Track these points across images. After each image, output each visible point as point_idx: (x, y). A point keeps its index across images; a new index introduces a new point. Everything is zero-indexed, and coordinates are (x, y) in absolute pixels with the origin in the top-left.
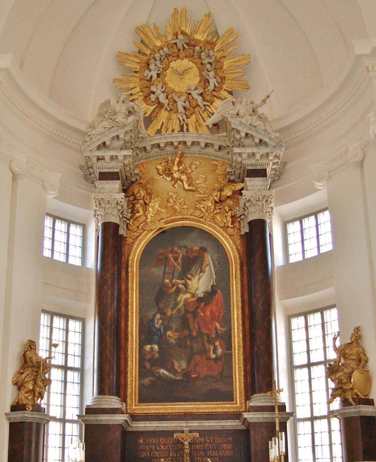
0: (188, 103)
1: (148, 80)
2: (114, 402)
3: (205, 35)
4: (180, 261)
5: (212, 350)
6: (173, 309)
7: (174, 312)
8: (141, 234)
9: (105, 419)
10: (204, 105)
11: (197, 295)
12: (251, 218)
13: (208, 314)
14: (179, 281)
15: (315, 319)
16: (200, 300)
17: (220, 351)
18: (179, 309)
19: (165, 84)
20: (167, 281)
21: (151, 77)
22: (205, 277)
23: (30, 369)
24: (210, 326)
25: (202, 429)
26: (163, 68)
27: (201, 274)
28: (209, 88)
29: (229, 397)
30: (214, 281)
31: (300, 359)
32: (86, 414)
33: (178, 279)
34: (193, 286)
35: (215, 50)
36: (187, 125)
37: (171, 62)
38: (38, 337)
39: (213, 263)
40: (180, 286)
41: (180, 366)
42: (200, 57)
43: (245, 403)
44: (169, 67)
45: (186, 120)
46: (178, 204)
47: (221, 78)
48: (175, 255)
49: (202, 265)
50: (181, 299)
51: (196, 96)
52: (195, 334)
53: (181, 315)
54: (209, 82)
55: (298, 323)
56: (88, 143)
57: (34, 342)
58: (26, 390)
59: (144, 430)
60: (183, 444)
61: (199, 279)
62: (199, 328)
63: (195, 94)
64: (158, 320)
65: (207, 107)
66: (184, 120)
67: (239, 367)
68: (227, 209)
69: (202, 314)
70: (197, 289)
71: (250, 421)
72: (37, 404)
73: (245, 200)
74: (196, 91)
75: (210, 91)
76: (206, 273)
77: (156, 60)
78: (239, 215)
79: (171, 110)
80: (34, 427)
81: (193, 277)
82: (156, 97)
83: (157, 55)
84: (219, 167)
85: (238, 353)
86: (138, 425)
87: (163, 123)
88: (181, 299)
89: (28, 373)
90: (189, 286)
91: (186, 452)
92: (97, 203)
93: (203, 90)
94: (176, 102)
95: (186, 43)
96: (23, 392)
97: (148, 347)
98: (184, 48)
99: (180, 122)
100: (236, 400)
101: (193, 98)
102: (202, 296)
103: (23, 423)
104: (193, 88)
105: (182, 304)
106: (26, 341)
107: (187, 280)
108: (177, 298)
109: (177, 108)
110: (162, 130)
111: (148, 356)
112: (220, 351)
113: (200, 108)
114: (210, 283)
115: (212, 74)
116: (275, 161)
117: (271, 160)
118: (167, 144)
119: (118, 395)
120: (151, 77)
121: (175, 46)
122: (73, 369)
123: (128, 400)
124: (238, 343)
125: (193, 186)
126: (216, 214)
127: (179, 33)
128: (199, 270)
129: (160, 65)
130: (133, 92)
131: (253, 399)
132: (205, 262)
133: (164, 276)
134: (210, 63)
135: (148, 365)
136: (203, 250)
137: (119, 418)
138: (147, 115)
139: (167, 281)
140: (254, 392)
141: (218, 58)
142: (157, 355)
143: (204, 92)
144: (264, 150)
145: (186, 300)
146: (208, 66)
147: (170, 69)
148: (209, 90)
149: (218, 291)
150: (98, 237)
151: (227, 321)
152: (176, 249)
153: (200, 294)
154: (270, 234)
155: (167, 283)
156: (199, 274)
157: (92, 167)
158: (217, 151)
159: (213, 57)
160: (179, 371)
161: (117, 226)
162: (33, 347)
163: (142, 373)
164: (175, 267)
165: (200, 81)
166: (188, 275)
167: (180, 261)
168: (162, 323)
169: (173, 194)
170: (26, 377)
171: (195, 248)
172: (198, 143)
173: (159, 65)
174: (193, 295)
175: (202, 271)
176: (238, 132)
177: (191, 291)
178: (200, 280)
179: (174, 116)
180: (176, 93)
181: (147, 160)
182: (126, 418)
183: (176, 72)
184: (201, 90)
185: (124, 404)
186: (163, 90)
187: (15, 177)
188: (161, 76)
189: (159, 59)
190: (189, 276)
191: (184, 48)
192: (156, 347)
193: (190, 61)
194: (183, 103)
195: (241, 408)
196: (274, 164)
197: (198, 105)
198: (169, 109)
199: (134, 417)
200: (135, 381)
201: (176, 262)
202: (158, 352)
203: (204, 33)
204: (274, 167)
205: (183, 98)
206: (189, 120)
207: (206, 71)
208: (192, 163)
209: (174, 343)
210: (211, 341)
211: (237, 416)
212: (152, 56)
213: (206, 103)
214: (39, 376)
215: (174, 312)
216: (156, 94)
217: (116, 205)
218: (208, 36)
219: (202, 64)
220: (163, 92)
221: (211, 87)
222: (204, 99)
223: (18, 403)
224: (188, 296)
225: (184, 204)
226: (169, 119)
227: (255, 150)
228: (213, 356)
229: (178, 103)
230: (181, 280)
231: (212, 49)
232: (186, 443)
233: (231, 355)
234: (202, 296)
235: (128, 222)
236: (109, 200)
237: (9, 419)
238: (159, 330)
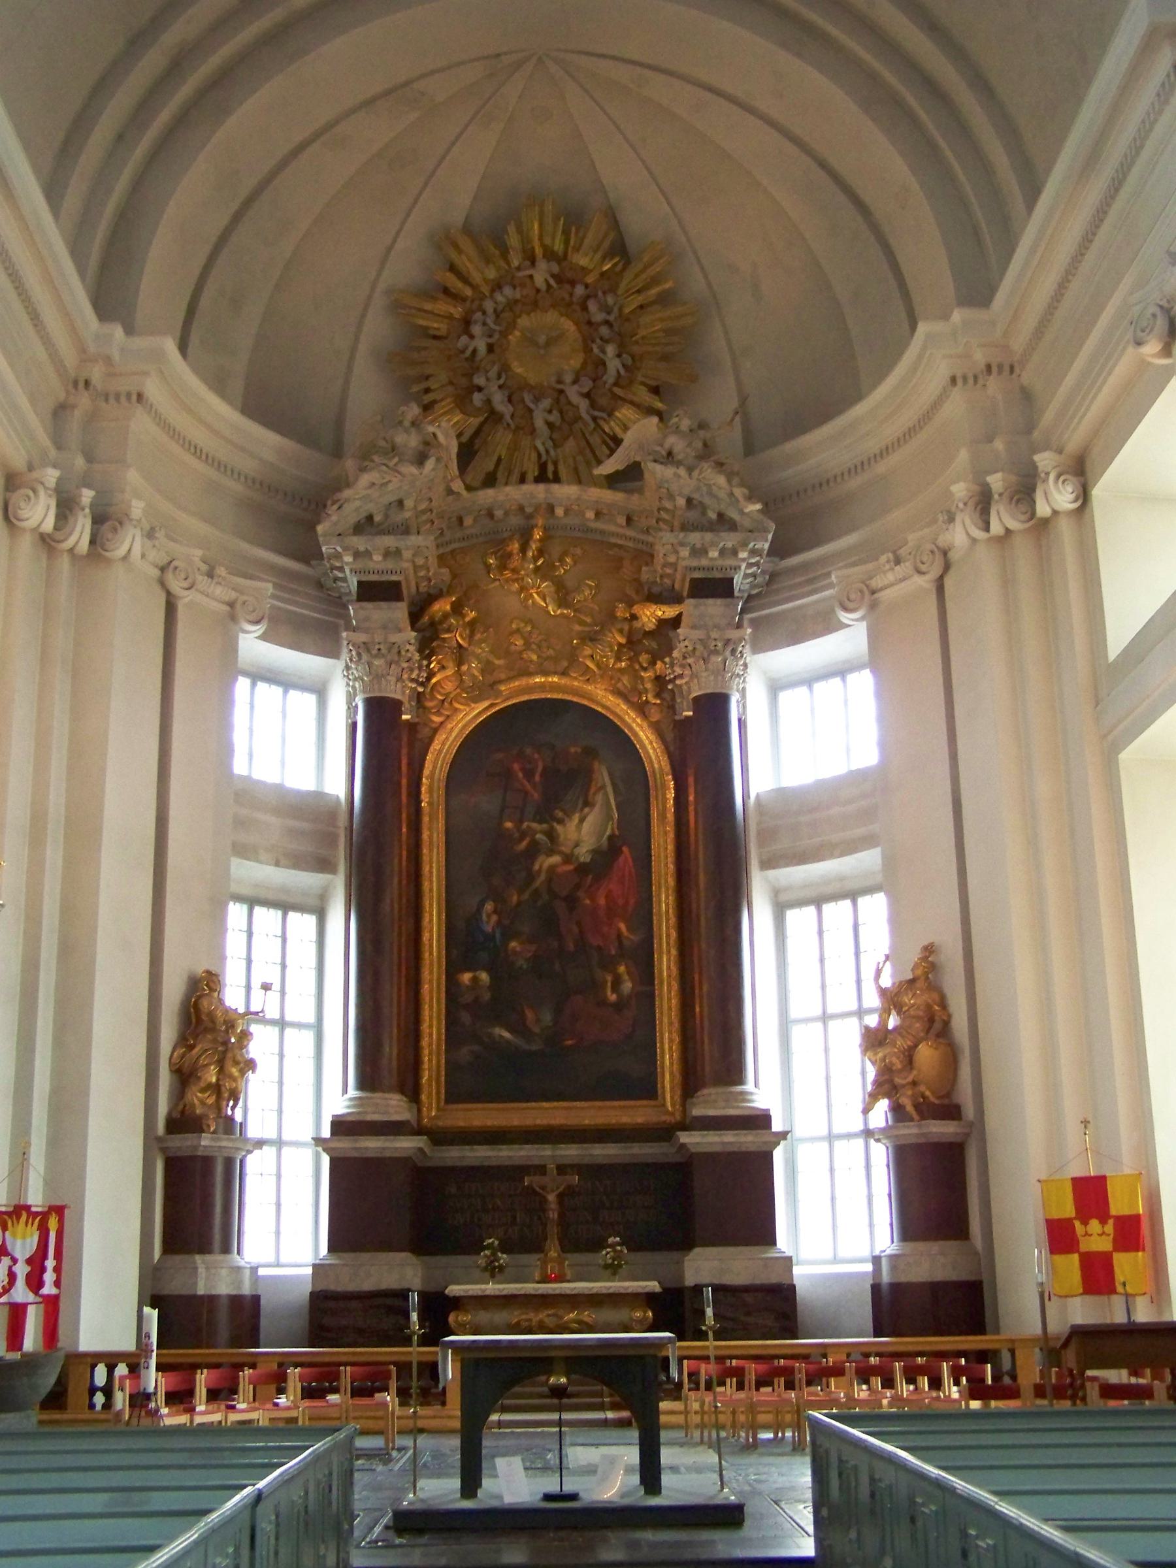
0: (559, 415)
1: (467, 359)
2: (395, 1107)
3: (598, 256)
4: (537, 778)
5: (609, 984)
6: (521, 891)
7: (526, 896)
8: (448, 717)
9: (372, 1145)
10: (595, 419)
11: (577, 858)
13: (602, 901)
14: (535, 825)
15: (838, 912)
16: (582, 869)
17: (627, 986)
18: (536, 890)
19: (505, 369)
20: (509, 825)
21: (474, 351)
22: (593, 818)
23: (209, 1037)
24: (605, 929)
25: (586, 1161)
26: (500, 332)
27: (586, 810)
28: (604, 378)
29: (648, 1090)
30: (615, 826)
31: (804, 1003)
32: (333, 1133)
33: (534, 821)
34: (569, 837)
35: (620, 292)
36: (555, 463)
37: (520, 316)
38: (223, 958)
39: (614, 785)
40: (538, 836)
41: (538, 1021)
42: (585, 308)
43: (684, 1105)
44: (514, 328)
45: (552, 453)
46: (534, 647)
47: (633, 357)
48: (528, 766)
49: (588, 790)
50: (541, 867)
51: (575, 399)
52: (571, 947)
53: (540, 903)
54: (604, 364)
55: (800, 919)
56: (334, 518)
57: (217, 975)
58: (202, 1084)
59: (459, 1164)
60: (546, 1200)
61: (582, 820)
62: (581, 932)
63: (573, 394)
64: (489, 916)
65: (601, 423)
66: (547, 452)
67: (671, 1024)
68: (644, 658)
69: (588, 902)
70: (577, 845)
71: (693, 1150)
72: (227, 1117)
73: (684, 650)
74: (576, 387)
75: (607, 386)
76: (597, 809)
77: (484, 313)
78: (672, 676)
79: (518, 428)
80: (219, 1169)
81: (568, 816)
82: (485, 398)
84: (626, 563)
85: (669, 992)
86: (447, 1155)
87: (499, 460)
88: (541, 867)
89: (206, 1045)
90: (558, 836)
91: (551, 1216)
92: (354, 653)
93: (591, 383)
94: (530, 411)
95: (553, 276)
96: (194, 1088)
97: (466, 977)
98: (549, 286)
99: (539, 456)
100: (664, 1098)
101: (569, 403)
102: (588, 860)
103: (193, 1158)
104: (568, 378)
105: (543, 877)
106: (200, 970)
107: (555, 824)
108: (533, 864)
109: (533, 424)
110: (499, 475)
111: (468, 998)
112: (627, 986)
113: (586, 424)
114: (605, 831)
115: (611, 350)
116: (753, 561)
117: (743, 560)
119: (401, 1090)
120: (474, 351)
121: (528, 281)
122: (299, 1026)
123: (424, 1097)
124: (669, 968)
125: (567, 606)
126: (621, 670)
127: (539, 251)
128: (581, 802)
129: (495, 324)
130: (431, 383)
131: (701, 1099)
132: (593, 783)
133: (502, 810)
134: (607, 323)
135: (465, 1017)
136: (590, 753)
137: (406, 1145)
138: (464, 439)
139: (509, 825)
140: (704, 1086)
141: (627, 310)
142: (487, 996)
143: (594, 387)
145: (552, 868)
146: (604, 331)
147: (517, 333)
148: (605, 383)
149: (625, 849)
150: (354, 725)
151: (645, 918)
152: (528, 751)
153: (583, 854)
154: (740, 720)
155: (508, 829)
156: (582, 810)
157: (341, 569)
158: (622, 527)
159: (616, 310)
160: (536, 1030)
161: (395, 706)
162: (212, 985)
163: (454, 1035)
164: (526, 793)
165: (584, 364)
166: (557, 811)
167: (537, 778)
168: (499, 923)
169: (522, 625)
170: (200, 1056)
171: (573, 750)
173: (492, 325)
174: (568, 859)
175: (587, 803)
177: (563, 849)
178: (586, 825)
179: (525, 442)
180: (531, 388)
181: (463, 544)
182: (421, 1145)
183: (530, 340)
184: (586, 385)
185: (415, 1106)
186: (501, 382)
188: (495, 347)
189: (492, 310)
190: (560, 814)
191: (549, 286)
192: (484, 976)
193: (562, 315)
194: (546, 414)
195: (672, 1114)
196: (750, 565)
197: (578, 418)
198: (513, 426)
199: (440, 1137)
200: (438, 1054)
201: (529, 781)
202: (490, 988)
203: (595, 251)
204: (750, 571)
205: (546, 403)
206: (559, 450)
207: (598, 341)
208: (565, 553)
209: (525, 967)
210: (608, 964)
211: (664, 1133)
212: (477, 303)
213: (596, 413)
214: (229, 1055)
215: (526, 896)
216: (486, 391)
217: (396, 658)
218: (604, 258)
219: (589, 323)
220: (500, 387)
221: (610, 377)
222: (593, 405)
223: (183, 1112)
224: (555, 859)
225: (548, 648)
226: (514, 447)
228: (613, 997)
229: (535, 414)
230: (540, 822)
231: (613, 290)
232: (551, 1197)
233: (651, 996)
234: (588, 860)
235: (421, 689)
236: (382, 647)
237: (163, 1150)
238: (490, 938)
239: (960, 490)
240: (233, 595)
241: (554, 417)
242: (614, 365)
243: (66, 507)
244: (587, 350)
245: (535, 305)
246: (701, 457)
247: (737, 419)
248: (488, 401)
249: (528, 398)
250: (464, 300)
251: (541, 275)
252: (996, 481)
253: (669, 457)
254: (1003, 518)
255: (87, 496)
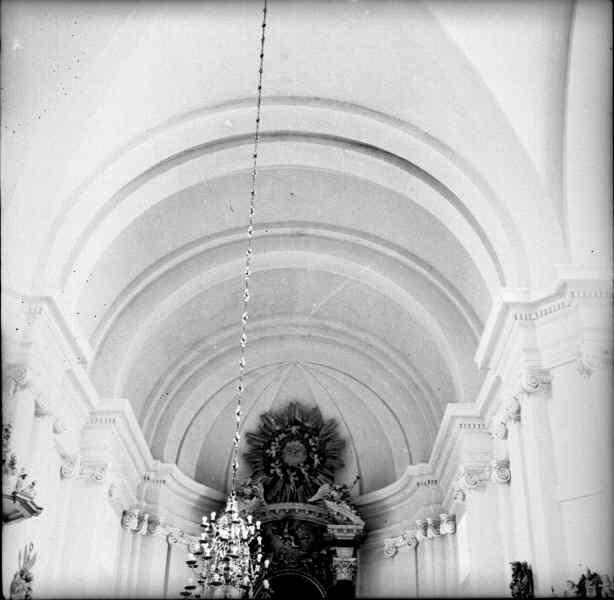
12: (339, 578)
19: (282, 461)
63: (303, 470)
83: (277, 439)
115: (316, 456)
118: (280, 511)
144: (350, 527)
146: (314, 449)
172: (304, 511)
176: (332, 510)
187: (169, 549)
227: (344, 527)
239: (419, 522)
240: (189, 542)
241: (297, 479)
242: (317, 461)
243: (141, 520)
244: (308, 455)
245: (292, 438)
246: (342, 499)
247: (357, 484)
248: (275, 472)
249: (288, 471)
250: (268, 436)
251: (294, 429)
252: (430, 521)
253: (332, 499)
254: (430, 532)
255: (147, 516)
